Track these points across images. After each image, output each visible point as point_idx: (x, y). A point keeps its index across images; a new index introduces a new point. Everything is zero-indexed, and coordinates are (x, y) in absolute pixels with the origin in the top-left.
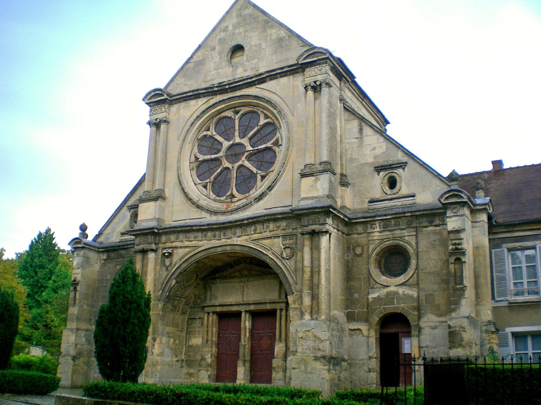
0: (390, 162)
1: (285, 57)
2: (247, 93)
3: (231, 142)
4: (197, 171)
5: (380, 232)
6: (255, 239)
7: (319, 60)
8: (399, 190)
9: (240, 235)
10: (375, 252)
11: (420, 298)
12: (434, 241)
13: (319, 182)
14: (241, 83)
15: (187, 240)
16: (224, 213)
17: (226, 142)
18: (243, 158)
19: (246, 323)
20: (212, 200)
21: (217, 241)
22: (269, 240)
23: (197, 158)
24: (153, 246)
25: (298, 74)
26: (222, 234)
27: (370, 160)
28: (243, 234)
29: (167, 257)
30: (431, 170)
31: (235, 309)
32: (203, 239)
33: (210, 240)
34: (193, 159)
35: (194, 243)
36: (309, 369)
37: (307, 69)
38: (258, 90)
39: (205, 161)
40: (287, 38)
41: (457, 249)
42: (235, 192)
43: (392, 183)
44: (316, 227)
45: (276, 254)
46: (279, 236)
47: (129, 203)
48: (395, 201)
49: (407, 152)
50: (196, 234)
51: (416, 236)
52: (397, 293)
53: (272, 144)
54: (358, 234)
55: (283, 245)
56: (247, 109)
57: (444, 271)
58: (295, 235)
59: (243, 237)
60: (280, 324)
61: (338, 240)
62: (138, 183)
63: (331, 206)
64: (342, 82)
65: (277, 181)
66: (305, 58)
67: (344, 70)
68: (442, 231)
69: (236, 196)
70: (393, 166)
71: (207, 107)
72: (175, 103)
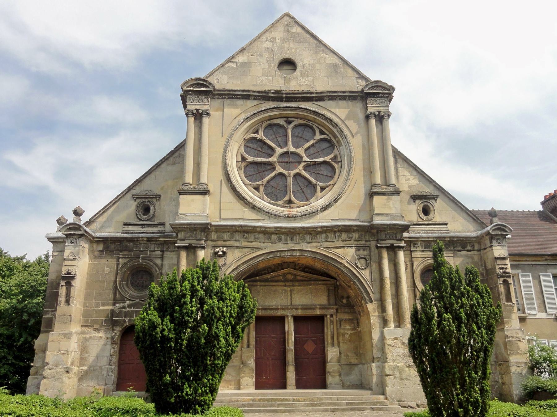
1: (341, 82)
3: (285, 150)
4: (244, 171)
5: (422, 251)
7: (382, 93)
8: (433, 218)
9: (309, 241)
10: (419, 268)
13: (391, 202)
15: (245, 240)
16: (287, 218)
18: (301, 167)
19: (290, 327)
21: (283, 245)
22: (342, 249)
23: (243, 159)
24: (203, 243)
26: (288, 238)
28: (313, 241)
29: (220, 256)
30: (460, 205)
31: (279, 313)
33: (275, 243)
34: (240, 159)
35: (254, 244)
36: (404, 376)
40: (342, 66)
41: (505, 272)
42: (293, 199)
43: (426, 211)
46: (353, 247)
47: (134, 191)
50: (257, 235)
53: (330, 159)
55: (357, 255)
56: (300, 121)
58: (368, 247)
62: (148, 172)
66: (369, 89)
68: (474, 256)
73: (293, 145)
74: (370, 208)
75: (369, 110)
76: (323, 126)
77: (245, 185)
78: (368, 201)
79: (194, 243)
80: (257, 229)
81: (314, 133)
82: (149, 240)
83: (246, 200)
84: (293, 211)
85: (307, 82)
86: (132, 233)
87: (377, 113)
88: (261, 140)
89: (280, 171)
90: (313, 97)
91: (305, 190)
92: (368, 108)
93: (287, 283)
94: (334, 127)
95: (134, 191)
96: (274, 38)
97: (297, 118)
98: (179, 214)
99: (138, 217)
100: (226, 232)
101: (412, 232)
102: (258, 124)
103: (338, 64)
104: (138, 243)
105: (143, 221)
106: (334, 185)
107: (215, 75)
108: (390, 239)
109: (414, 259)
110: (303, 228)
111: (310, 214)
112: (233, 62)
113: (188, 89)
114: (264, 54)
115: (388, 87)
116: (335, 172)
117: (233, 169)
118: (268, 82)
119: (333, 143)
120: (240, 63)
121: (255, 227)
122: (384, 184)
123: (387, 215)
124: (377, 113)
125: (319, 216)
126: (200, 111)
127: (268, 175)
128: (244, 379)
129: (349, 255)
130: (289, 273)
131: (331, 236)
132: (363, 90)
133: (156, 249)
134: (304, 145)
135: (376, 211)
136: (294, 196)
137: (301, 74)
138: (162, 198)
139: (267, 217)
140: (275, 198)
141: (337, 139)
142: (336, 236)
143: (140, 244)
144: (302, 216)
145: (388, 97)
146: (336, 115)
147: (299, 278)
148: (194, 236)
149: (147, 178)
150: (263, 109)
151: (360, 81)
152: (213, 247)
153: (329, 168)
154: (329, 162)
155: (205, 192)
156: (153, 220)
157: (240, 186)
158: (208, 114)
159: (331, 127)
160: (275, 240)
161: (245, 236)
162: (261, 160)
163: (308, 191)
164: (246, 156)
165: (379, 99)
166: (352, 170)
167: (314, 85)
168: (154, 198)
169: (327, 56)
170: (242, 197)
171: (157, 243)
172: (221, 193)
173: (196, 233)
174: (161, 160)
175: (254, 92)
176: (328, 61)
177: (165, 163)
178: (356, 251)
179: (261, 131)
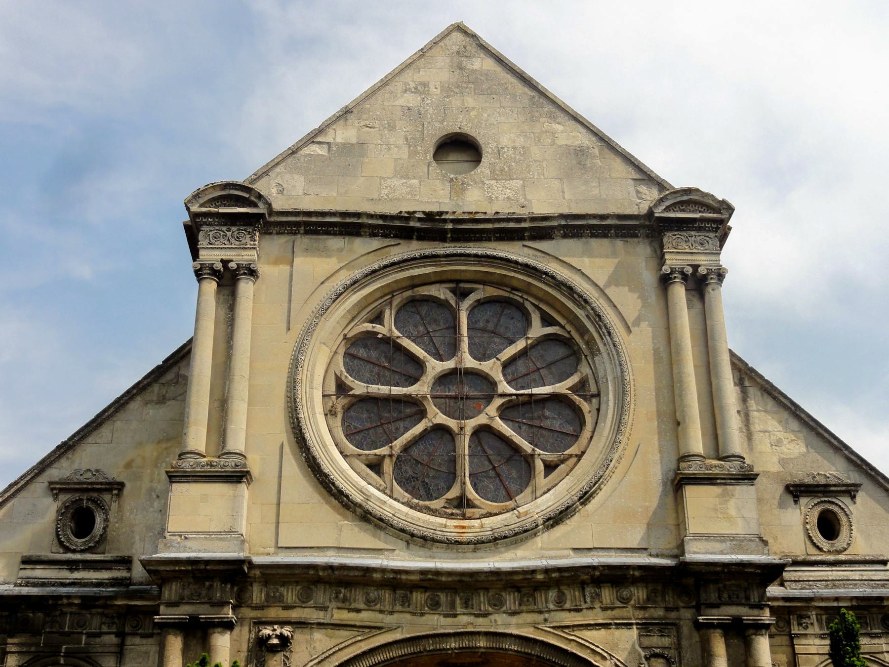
1: (596, 192)
2: (490, 252)
3: (450, 364)
4: (343, 419)
7: (702, 220)
8: (849, 544)
9: (515, 607)
13: (732, 503)
14: (490, 226)
16: (453, 545)
18: (492, 409)
20: (403, 503)
21: (442, 619)
22: (603, 632)
23: (342, 387)
24: (229, 613)
25: (636, 240)
26: (458, 601)
28: (524, 608)
29: (274, 649)
33: (422, 615)
34: (332, 388)
35: (366, 617)
37: (671, 234)
38: (531, 252)
42: (471, 493)
46: (631, 624)
47: (55, 473)
49: (859, 462)
50: (373, 594)
53: (569, 389)
55: (644, 648)
59: (524, 615)
62: (93, 421)
65: (602, 483)
66: (667, 209)
69: (477, 503)
72: (278, 233)
73: (471, 353)
74: (677, 517)
75: (668, 262)
77: (345, 457)
78: (670, 499)
79: (205, 613)
80: (374, 575)
81: (528, 323)
82: (88, 602)
83: (347, 496)
84: (470, 527)
85: (508, 191)
86: (43, 585)
87: (689, 270)
88: (389, 338)
90: (525, 229)
91: (504, 470)
92: (667, 256)
94: (580, 306)
95: (55, 473)
96: (425, 85)
97: (484, 283)
98: (167, 535)
99: (61, 543)
100: (290, 583)
101: (793, 585)
102: (382, 297)
103: (588, 148)
104: (58, 613)
105: (74, 551)
106: (579, 457)
107: (272, 174)
108: (730, 603)
110: (496, 574)
111: (516, 534)
112: (319, 143)
113: (204, 210)
114: (399, 124)
115: (716, 205)
116: (582, 423)
117: (314, 414)
118: (409, 193)
119: (576, 348)
120: (337, 144)
121: (368, 570)
122: (712, 453)
123: (721, 538)
124: (689, 270)
125: (542, 540)
126: (233, 265)
127: (407, 430)
129: (621, 646)
131: (571, 595)
132: (650, 213)
133: (105, 629)
134: (500, 351)
135: (694, 526)
137: (493, 171)
138: (126, 491)
139: (403, 544)
141: (586, 337)
142: (587, 594)
143: (63, 614)
144: (496, 541)
145: (718, 228)
146: (583, 274)
148: (204, 592)
149: (90, 439)
150: (396, 259)
151: (643, 189)
152: (255, 623)
153: (567, 412)
154: (565, 397)
155: (239, 477)
156: (101, 549)
157: (333, 461)
158: (252, 273)
159: (570, 305)
160: (422, 607)
161: (342, 595)
162: (387, 392)
163: (510, 473)
164: (350, 380)
165: (693, 233)
166: (628, 418)
167: (526, 199)
168: (106, 490)
169: (560, 128)
170: (336, 488)
171: (106, 612)
172: (280, 477)
173: (211, 586)
174: (128, 392)
175: (371, 216)
176: (562, 141)
177: (139, 399)
178: (640, 636)
179: (389, 317)
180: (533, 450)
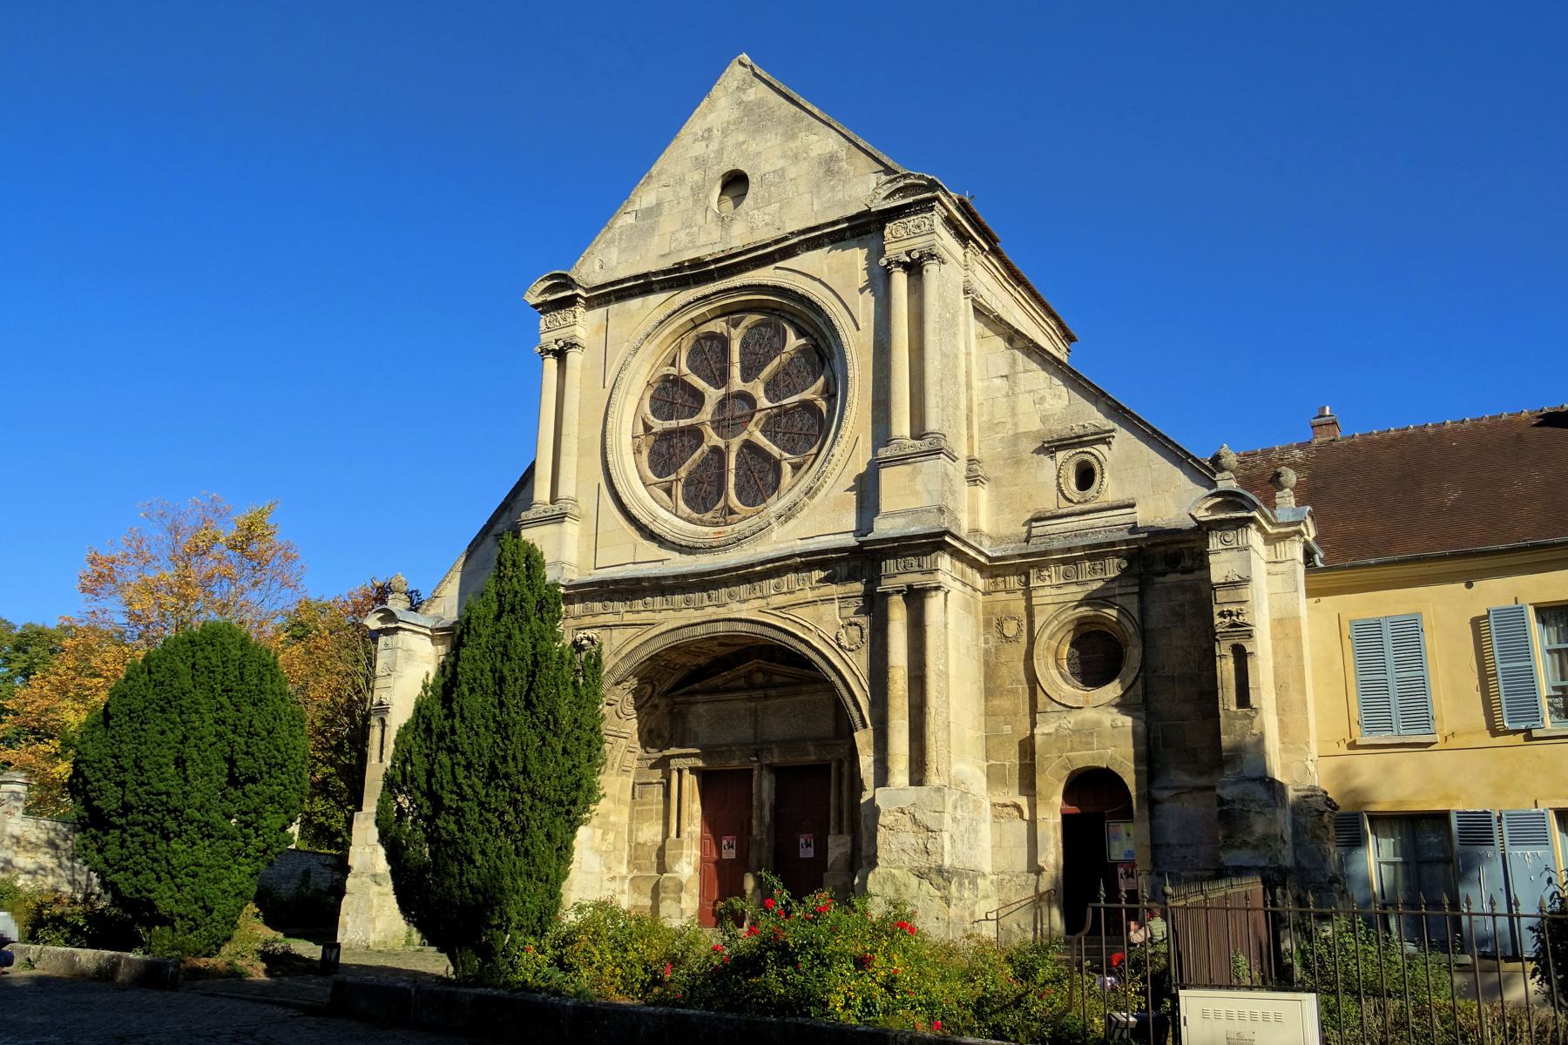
0: (1078, 431)
1: (840, 195)
3: (723, 391)
5: (1058, 587)
6: (779, 605)
11: (1152, 735)
12: (1181, 605)
13: (920, 478)
16: (710, 549)
17: (712, 389)
18: (751, 427)
22: (811, 609)
23: (647, 428)
25: (870, 236)
27: (1035, 425)
28: (753, 596)
32: (665, 607)
33: (681, 610)
34: (641, 429)
35: (645, 617)
39: (667, 435)
40: (843, 154)
41: (1234, 625)
43: (1086, 477)
44: (916, 579)
45: (826, 638)
46: (833, 599)
48: (1091, 516)
51: (1141, 596)
52: (1098, 723)
54: (1008, 592)
57: (1205, 673)
60: (840, 792)
61: (967, 607)
63: (947, 532)
64: (968, 250)
67: (972, 225)
69: (737, 510)
70: (1085, 439)
71: (669, 312)
76: (801, 318)
84: (724, 532)
89: (711, 444)
92: (887, 247)
93: (754, 694)
109: (1037, 610)
121: (638, 580)
128: (664, 903)
129: (825, 619)
130: (760, 670)
136: (739, 496)
137: (756, 202)
140: (702, 508)
144: (738, 541)
147: (778, 679)
169: (814, 138)
175: (655, 274)
180: (781, 455)
